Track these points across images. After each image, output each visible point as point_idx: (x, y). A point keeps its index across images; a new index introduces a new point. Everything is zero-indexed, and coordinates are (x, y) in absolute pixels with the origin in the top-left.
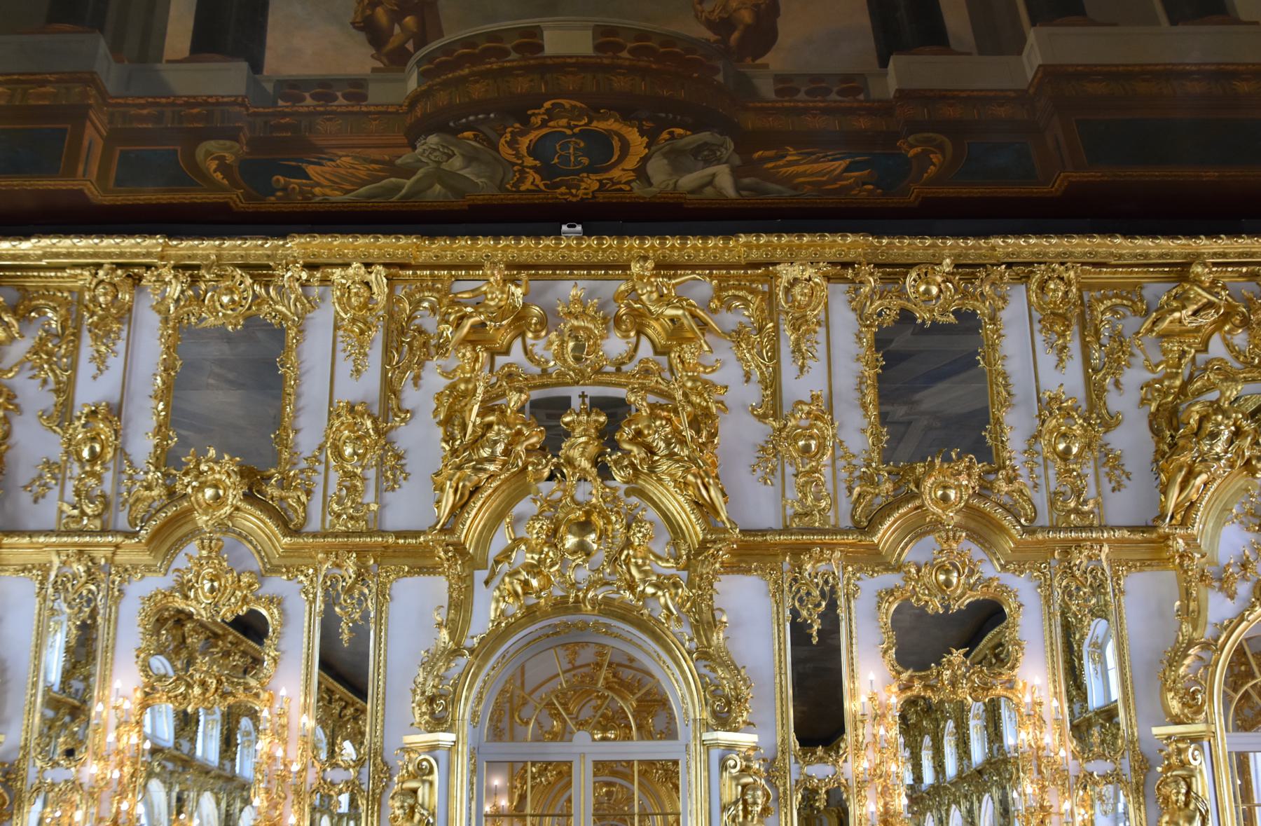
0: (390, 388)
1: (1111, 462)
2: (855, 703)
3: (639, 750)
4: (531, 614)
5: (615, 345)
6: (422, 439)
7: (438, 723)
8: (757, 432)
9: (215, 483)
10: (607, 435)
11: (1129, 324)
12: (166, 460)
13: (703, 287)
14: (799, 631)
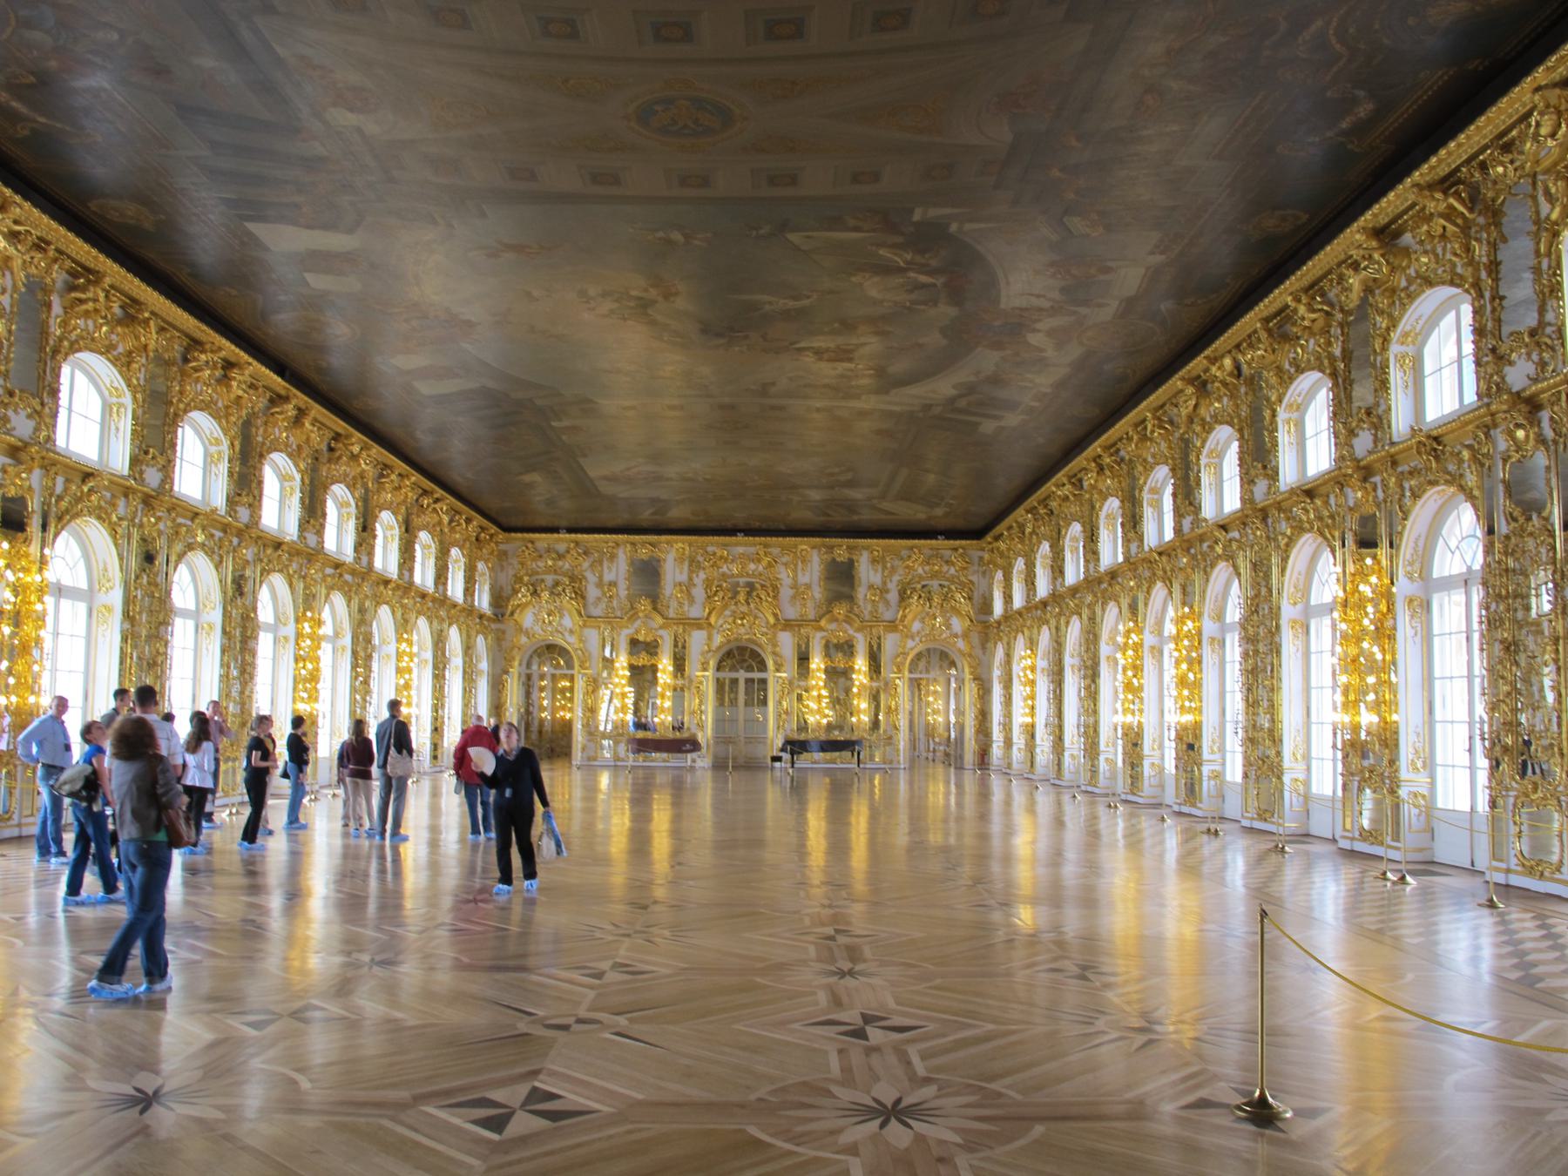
0: (691, 579)
1: (887, 603)
2: (813, 666)
3: (756, 675)
4: (729, 641)
5: (752, 566)
6: (699, 592)
7: (705, 670)
8: (791, 592)
9: (644, 605)
10: (749, 594)
11: (897, 563)
12: (629, 597)
13: (775, 551)
14: (799, 646)
